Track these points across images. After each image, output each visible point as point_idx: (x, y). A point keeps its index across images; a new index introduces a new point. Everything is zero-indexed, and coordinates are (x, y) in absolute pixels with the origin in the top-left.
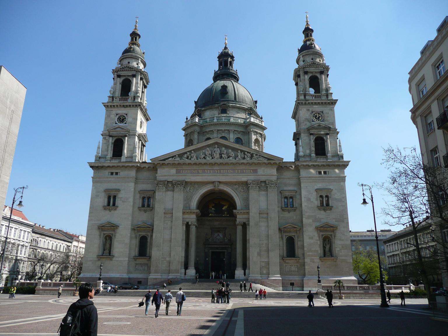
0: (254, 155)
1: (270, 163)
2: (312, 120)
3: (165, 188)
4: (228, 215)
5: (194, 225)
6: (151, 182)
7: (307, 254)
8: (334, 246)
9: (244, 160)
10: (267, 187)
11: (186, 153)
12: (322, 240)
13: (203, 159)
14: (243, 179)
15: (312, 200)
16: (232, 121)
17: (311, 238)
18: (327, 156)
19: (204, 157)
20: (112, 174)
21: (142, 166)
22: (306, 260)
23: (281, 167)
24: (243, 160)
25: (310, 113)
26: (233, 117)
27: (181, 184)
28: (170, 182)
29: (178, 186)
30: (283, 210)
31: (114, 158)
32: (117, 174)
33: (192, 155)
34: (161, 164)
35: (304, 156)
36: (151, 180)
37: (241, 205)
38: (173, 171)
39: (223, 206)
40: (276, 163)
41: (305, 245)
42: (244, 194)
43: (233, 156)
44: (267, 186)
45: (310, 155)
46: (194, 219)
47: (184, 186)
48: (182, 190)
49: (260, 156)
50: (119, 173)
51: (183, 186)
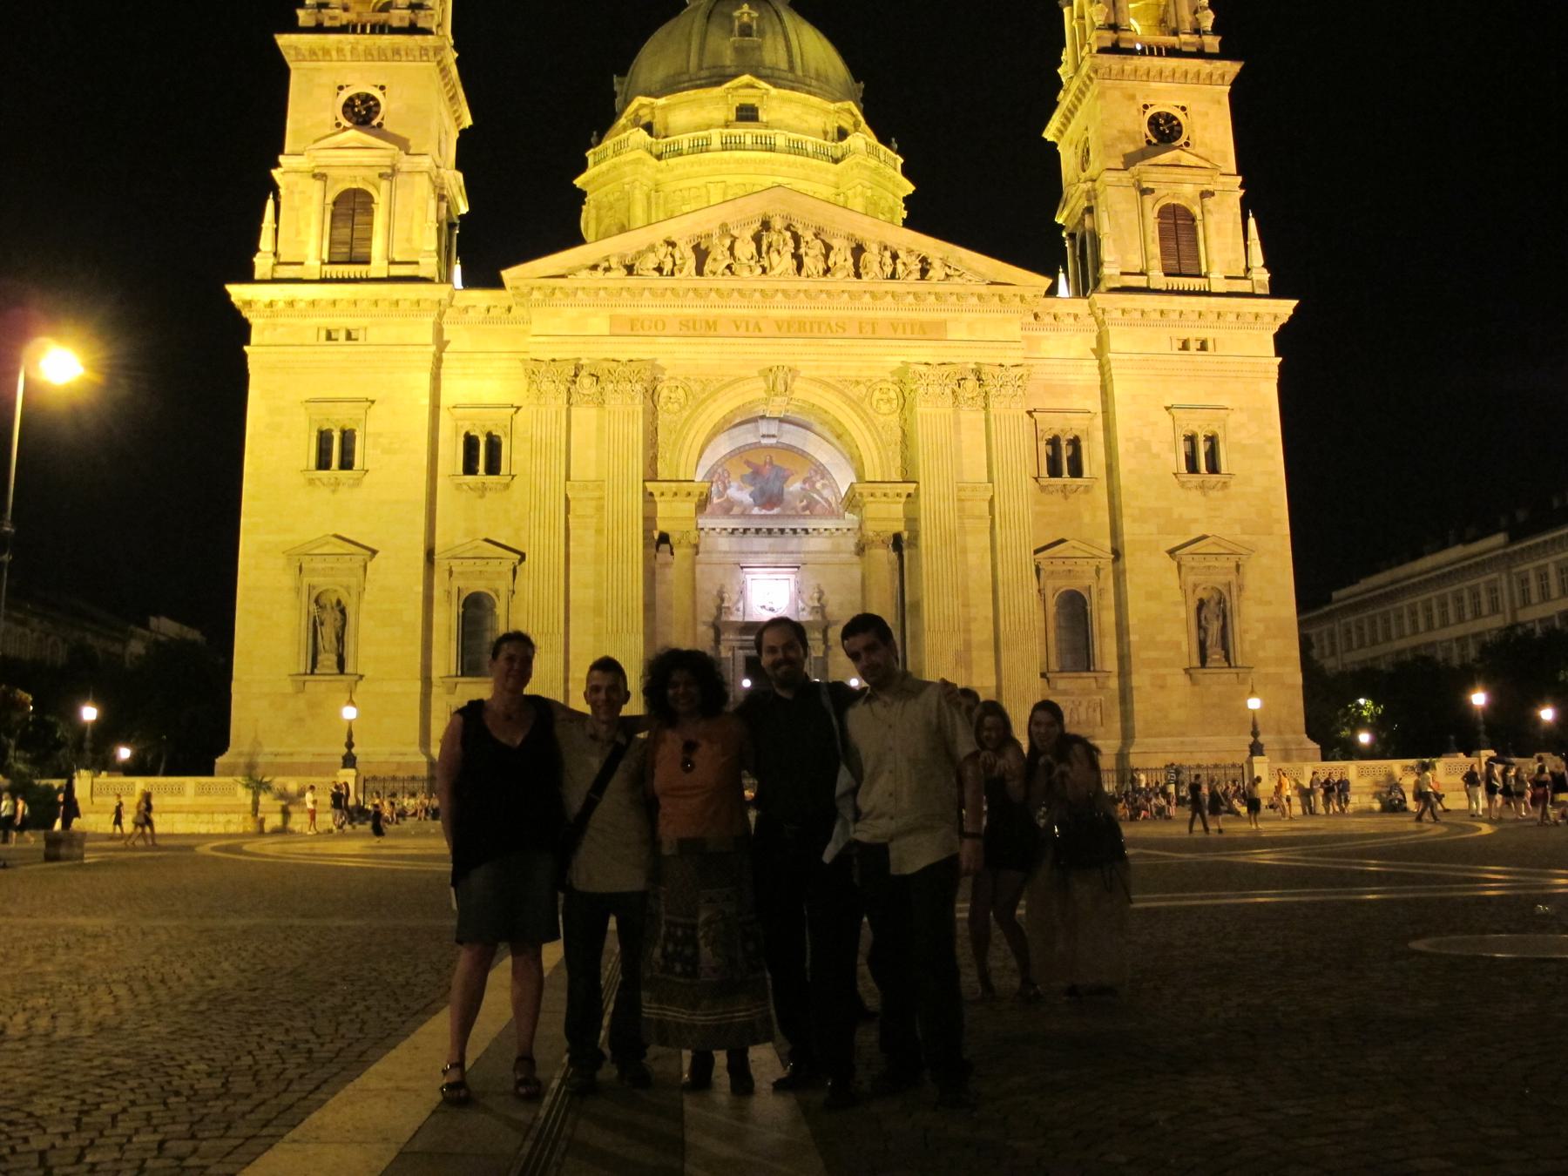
0: (937, 264)
2: (1146, 136)
7: (1139, 655)
8: (1237, 625)
11: (652, 248)
12: (1193, 605)
14: (889, 358)
15: (1155, 450)
17: (1151, 596)
19: (729, 267)
22: (1137, 680)
25: (1138, 110)
30: (1043, 489)
33: (677, 256)
41: (1130, 623)
48: (637, 401)
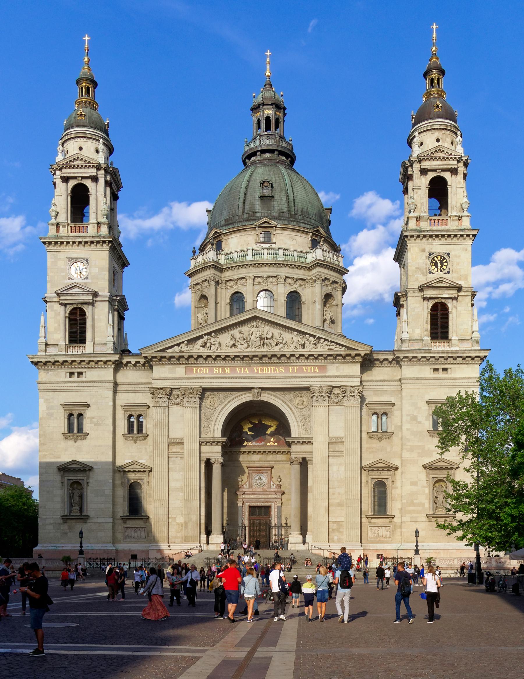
1: (349, 355)
3: (166, 400)
4: (276, 444)
5: (220, 463)
6: (143, 389)
9: (304, 350)
10: (344, 397)
13: (231, 347)
16: (283, 259)
18: (451, 340)
19: (234, 345)
20: (71, 374)
21: (125, 361)
23: (369, 360)
24: (302, 350)
26: (284, 249)
27: (195, 393)
28: (176, 390)
29: (191, 396)
31: (71, 346)
32: (80, 374)
34: (159, 358)
35: (409, 340)
36: (140, 386)
37: (298, 429)
38: (180, 370)
39: (268, 427)
40: (359, 355)
42: (304, 410)
43: (284, 342)
44: (344, 395)
45: (421, 337)
46: (219, 453)
47: (200, 396)
49: (331, 342)
50: (84, 374)
51: (198, 397)
